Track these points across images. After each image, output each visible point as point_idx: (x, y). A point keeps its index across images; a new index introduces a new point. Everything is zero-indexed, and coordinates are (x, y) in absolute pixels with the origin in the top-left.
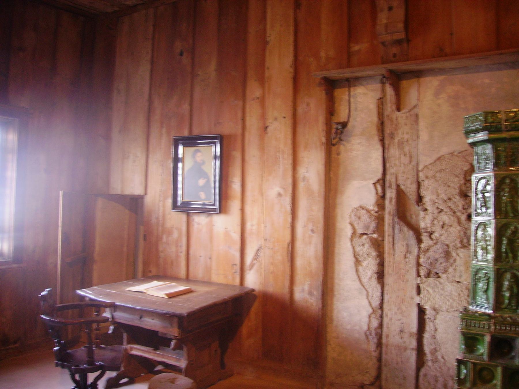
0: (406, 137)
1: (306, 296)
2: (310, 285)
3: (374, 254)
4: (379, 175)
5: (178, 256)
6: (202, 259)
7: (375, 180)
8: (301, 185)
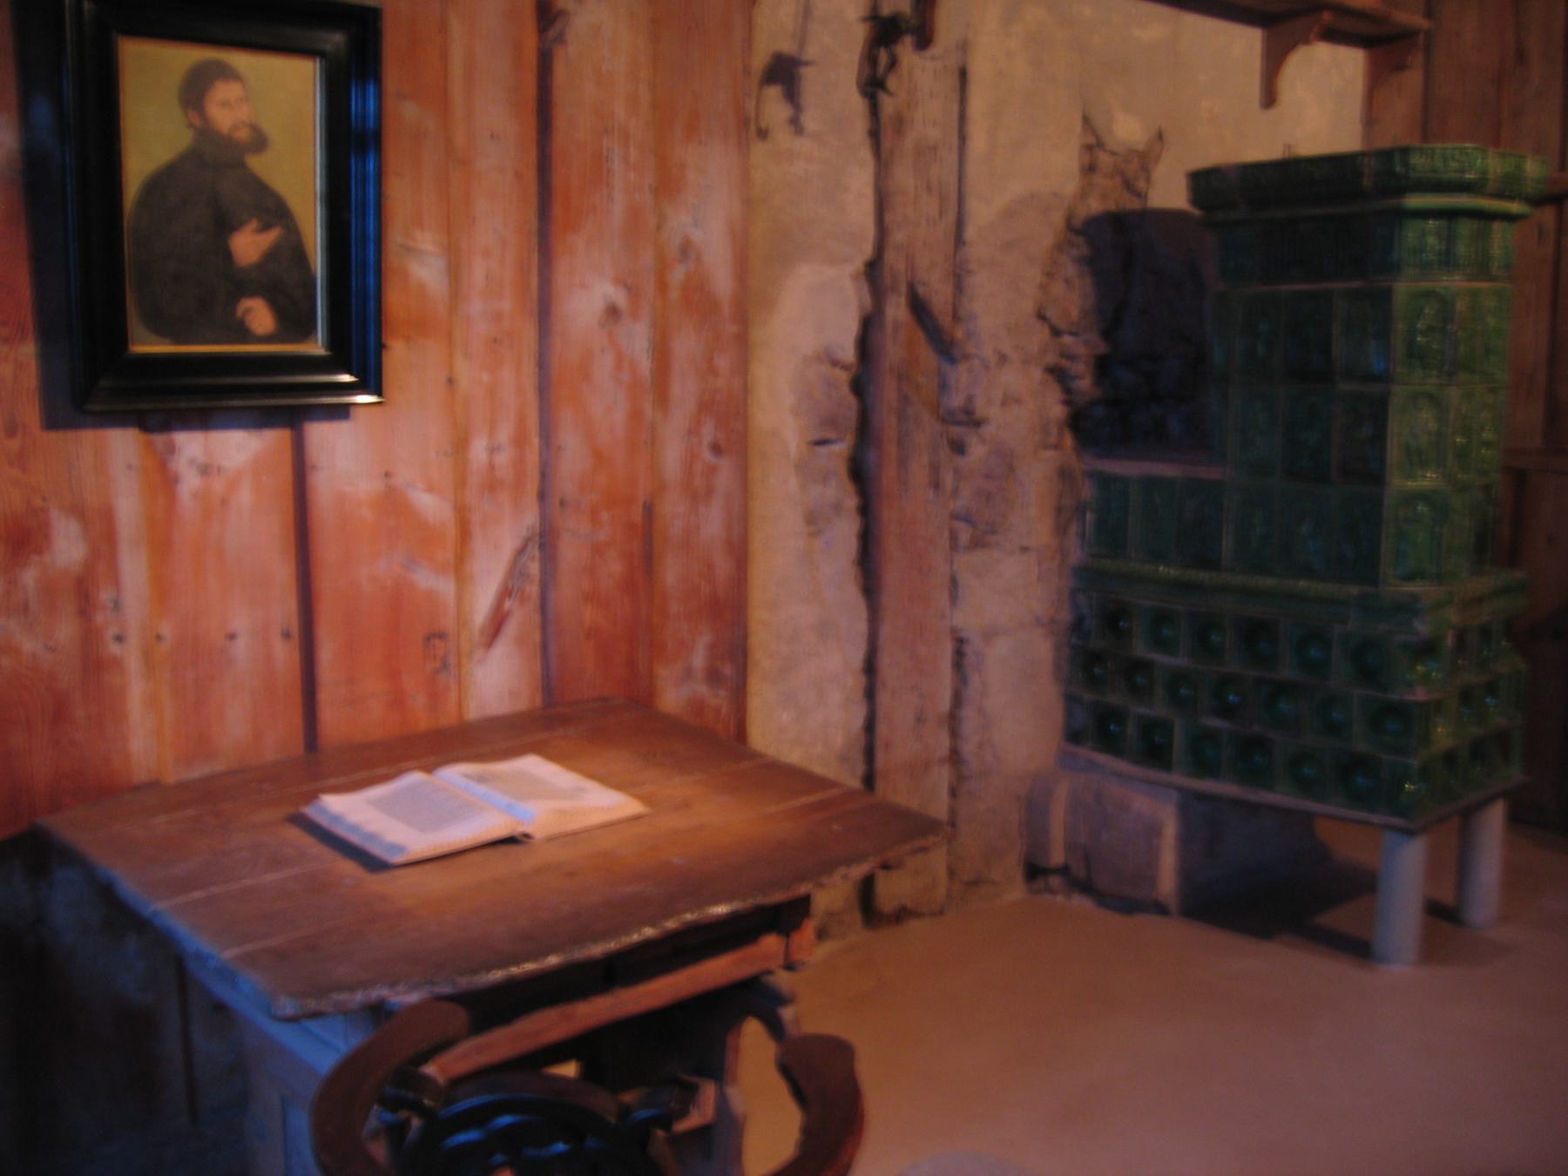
0: (934, 134)
1: (702, 689)
2: (712, 647)
3: (851, 502)
4: (868, 250)
5: (95, 663)
6: (242, 649)
7: (858, 263)
8: (677, 275)
